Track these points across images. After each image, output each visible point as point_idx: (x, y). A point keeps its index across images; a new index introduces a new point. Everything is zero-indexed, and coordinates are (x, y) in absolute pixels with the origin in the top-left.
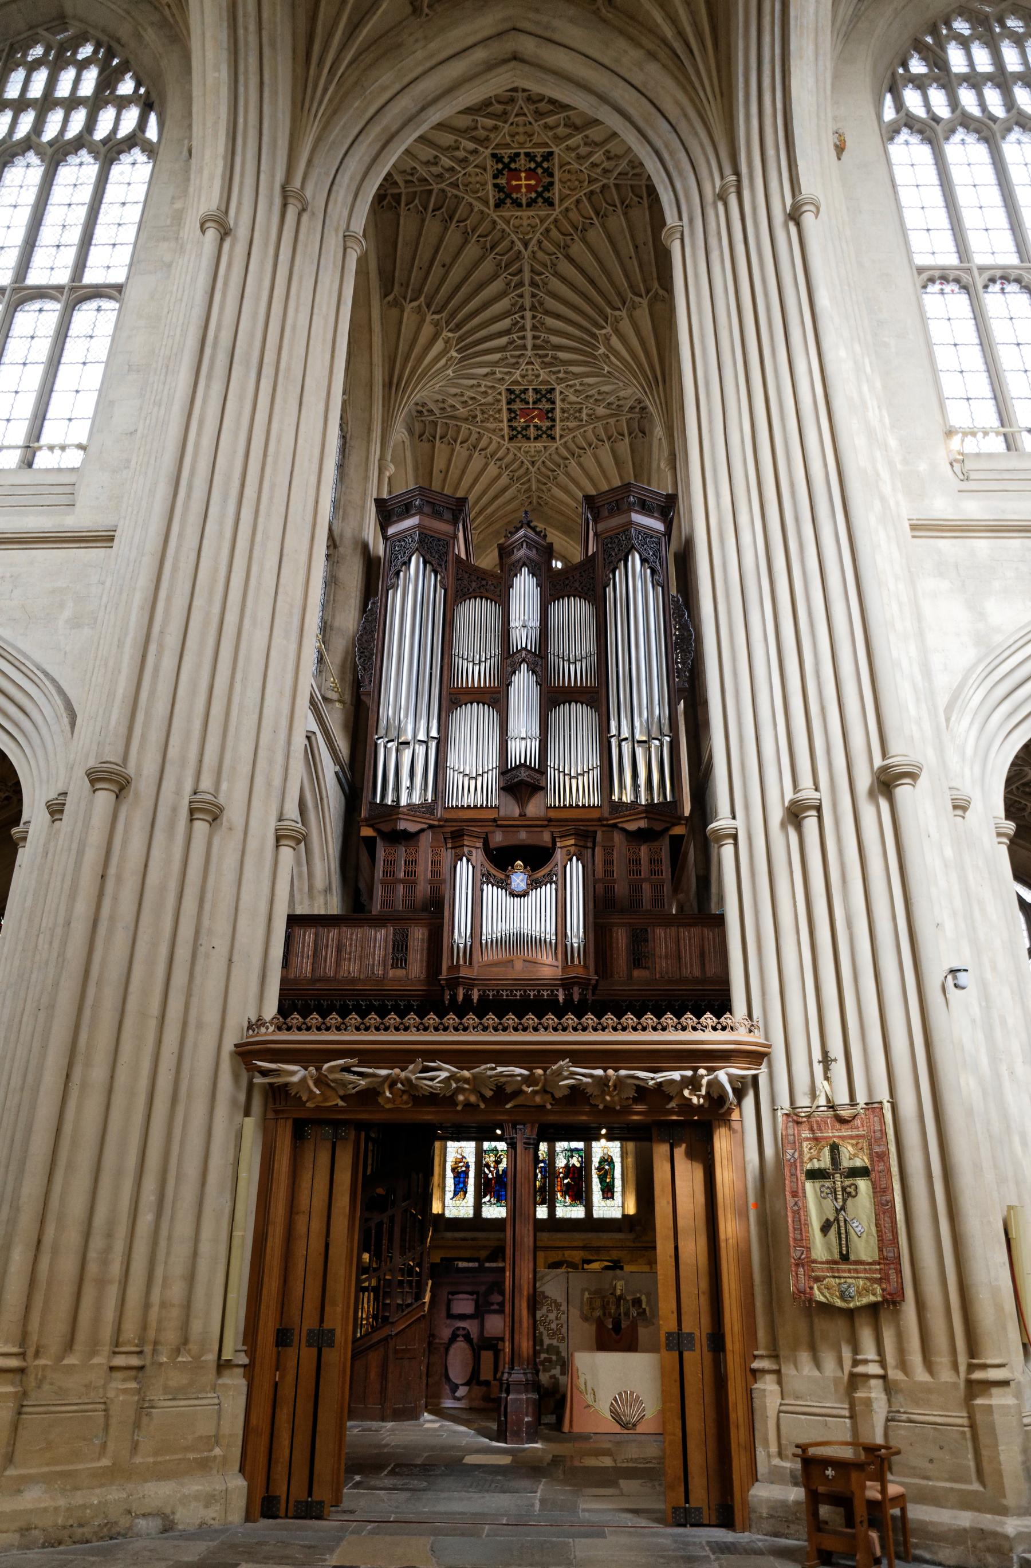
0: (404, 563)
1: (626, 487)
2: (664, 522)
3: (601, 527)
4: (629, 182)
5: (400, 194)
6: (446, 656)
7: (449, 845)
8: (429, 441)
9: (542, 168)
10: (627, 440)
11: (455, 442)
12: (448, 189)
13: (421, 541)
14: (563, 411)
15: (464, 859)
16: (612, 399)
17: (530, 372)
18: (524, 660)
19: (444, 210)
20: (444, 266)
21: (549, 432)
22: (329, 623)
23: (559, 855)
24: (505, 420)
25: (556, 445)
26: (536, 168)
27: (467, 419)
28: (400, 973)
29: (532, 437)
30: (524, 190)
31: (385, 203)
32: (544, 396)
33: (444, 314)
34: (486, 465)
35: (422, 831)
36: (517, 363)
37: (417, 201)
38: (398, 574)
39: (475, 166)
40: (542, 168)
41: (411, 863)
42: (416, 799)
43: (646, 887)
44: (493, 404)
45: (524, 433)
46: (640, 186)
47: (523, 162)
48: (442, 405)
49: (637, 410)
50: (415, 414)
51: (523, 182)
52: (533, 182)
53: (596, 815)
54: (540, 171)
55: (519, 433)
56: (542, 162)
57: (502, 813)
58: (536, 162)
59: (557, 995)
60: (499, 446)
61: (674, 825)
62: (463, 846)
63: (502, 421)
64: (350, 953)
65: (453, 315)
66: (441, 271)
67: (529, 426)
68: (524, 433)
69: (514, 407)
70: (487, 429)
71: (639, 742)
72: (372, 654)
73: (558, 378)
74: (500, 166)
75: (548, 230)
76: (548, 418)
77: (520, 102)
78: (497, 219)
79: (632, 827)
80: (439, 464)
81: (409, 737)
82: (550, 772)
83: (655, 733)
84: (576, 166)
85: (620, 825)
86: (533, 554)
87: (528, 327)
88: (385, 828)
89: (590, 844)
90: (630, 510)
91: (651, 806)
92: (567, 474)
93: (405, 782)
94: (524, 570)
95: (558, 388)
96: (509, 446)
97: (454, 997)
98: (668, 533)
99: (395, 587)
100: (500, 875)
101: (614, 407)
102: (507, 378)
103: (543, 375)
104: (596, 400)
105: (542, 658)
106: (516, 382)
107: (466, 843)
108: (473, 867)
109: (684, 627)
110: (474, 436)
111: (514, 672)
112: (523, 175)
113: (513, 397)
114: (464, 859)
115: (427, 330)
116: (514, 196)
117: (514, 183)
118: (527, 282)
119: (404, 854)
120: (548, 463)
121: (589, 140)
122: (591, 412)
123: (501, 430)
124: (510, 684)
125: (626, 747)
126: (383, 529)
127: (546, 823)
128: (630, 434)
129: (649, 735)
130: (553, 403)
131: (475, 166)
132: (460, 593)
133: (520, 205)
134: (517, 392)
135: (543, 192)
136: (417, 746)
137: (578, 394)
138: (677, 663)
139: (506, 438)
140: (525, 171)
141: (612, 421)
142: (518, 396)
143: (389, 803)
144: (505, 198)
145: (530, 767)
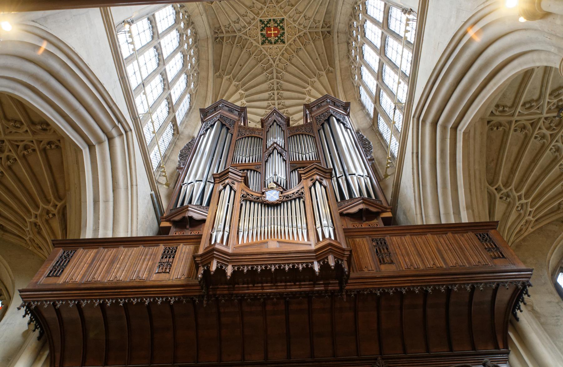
1: (326, 97)
4: (315, 30)
5: (223, 37)
9: (280, 26)
12: (243, 35)
18: (275, 148)
19: (241, 44)
20: (241, 66)
22: (168, 155)
26: (277, 26)
30: (273, 35)
31: (218, 40)
33: (240, 83)
37: (230, 40)
38: (207, 130)
39: (253, 26)
40: (280, 26)
46: (319, 32)
47: (272, 23)
51: (273, 32)
52: (276, 32)
54: (279, 27)
56: (280, 23)
58: (277, 23)
65: (244, 85)
66: (239, 67)
74: (263, 26)
75: (283, 54)
78: (262, 49)
84: (294, 25)
85: (345, 212)
87: (276, 99)
112: (272, 29)
115: (232, 88)
116: (269, 39)
117: (269, 32)
118: (275, 77)
121: (298, 11)
131: (253, 26)
133: (271, 43)
140: (273, 27)
144: (266, 39)
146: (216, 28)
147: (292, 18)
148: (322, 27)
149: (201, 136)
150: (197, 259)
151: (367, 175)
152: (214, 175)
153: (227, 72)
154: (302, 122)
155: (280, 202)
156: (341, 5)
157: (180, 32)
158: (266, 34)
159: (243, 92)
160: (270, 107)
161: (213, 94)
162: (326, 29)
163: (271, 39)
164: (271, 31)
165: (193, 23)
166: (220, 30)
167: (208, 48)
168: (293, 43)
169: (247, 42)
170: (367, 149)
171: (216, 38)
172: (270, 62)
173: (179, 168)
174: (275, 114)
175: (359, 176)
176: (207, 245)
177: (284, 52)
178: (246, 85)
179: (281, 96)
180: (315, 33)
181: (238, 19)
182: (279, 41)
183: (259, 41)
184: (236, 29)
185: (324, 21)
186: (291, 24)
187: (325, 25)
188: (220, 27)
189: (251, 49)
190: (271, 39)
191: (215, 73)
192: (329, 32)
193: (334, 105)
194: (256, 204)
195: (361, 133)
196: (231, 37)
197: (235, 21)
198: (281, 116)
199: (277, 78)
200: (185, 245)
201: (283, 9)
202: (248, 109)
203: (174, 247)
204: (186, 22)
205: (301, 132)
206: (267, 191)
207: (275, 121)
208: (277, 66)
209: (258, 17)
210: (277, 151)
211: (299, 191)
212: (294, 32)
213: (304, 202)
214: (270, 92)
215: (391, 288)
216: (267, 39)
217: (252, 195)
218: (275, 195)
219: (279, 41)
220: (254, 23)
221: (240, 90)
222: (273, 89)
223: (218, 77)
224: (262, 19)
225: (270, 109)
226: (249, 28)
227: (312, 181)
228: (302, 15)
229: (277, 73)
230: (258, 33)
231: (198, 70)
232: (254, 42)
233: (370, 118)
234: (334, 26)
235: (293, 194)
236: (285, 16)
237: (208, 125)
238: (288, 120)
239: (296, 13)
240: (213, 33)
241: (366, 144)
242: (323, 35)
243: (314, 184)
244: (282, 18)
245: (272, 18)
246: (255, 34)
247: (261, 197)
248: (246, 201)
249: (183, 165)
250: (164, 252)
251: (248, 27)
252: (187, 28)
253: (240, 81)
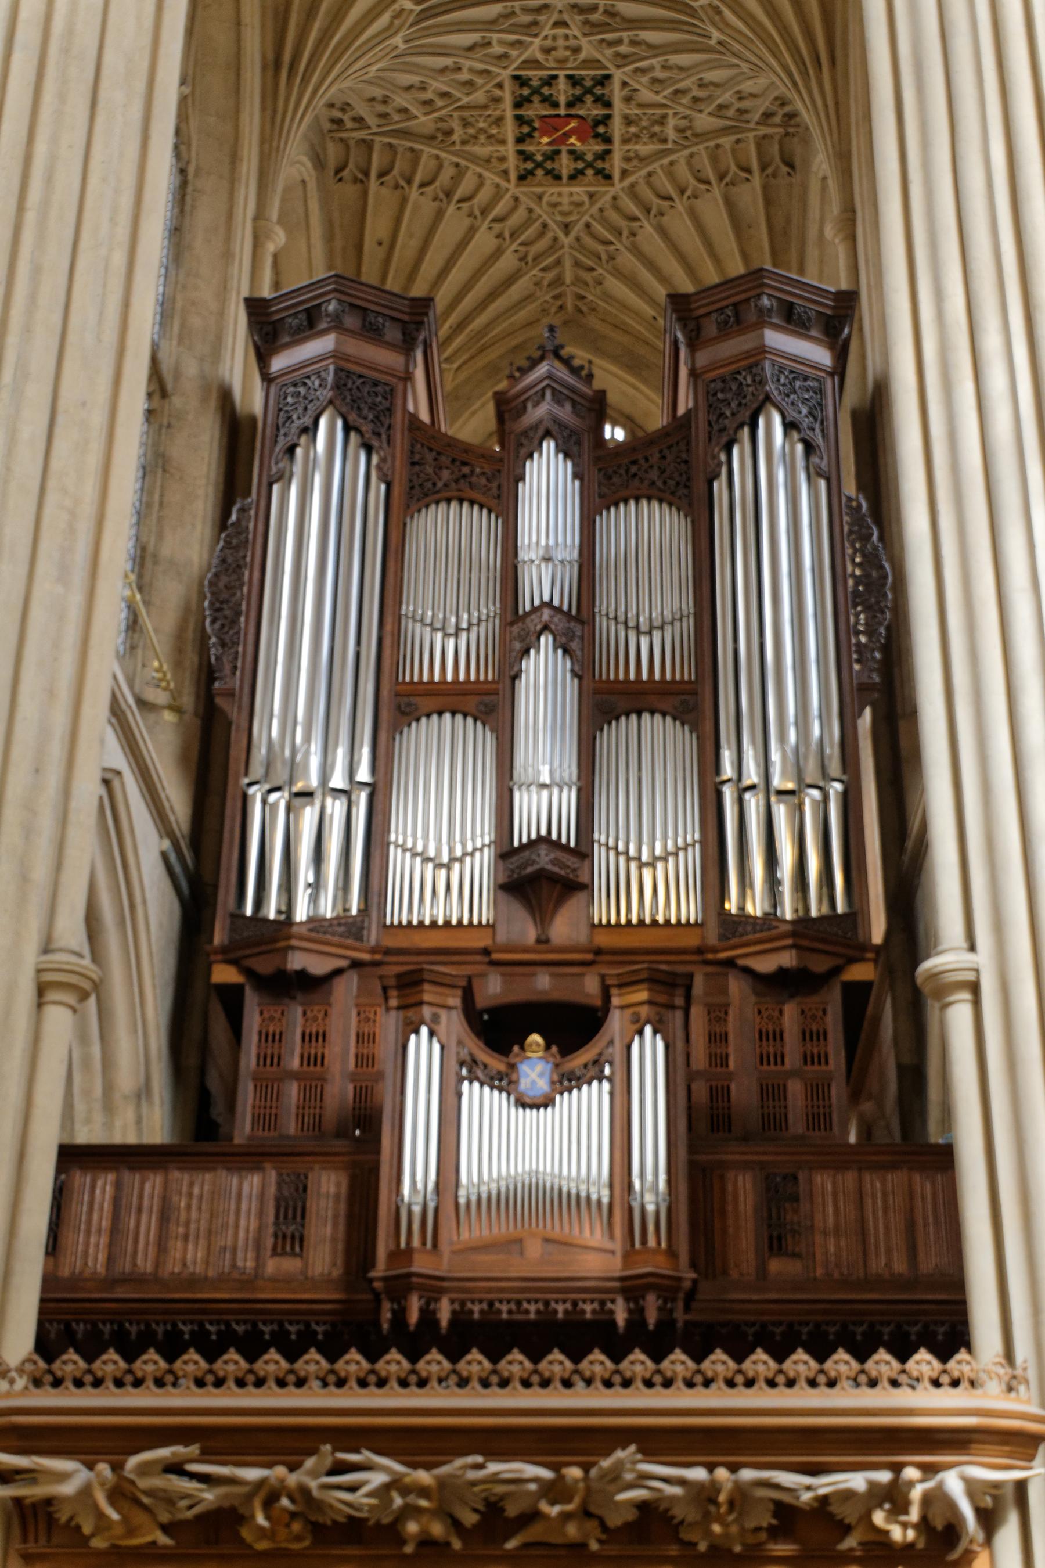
0: (305, 430)
1: (755, 277)
2: (831, 347)
3: (703, 358)
6: (389, 620)
7: (393, 1002)
8: (356, 180)
10: (757, 180)
11: (409, 182)
13: (338, 386)
14: (628, 121)
15: (424, 1031)
16: (726, 97)
17: (561, 42)
18: (546, 628)
21: (599, 165)
22: (151, 548)
23: (616, 1022)
24: (510, 139)
25: (612, 191)
27: (433, 138)
28: (290, 1265)
29: (565, 173)
32: (589, 91)
34: (472, 231)
35: (338, 972)
36: (535, 23)
38: (291, 450)
41: (315, 1037)
42: (327, 909)
43: (795, 1088)
44: (485, 107)
45: (549, 165)
48: (381, 108)
49: (777, 119)
50: (327, 126)
53: (691, 940)
55: (539, 165)
57: (502, 937)
59: (612, 1312)
60: (498, 193)
61: (852, 961)
62: (420, 1003)
63: (503, 142)
64: (187, 1224)
67: (558, 152)
68: (549, 165)
69: (528, 112)
70: (474, 159)
71: (780, 793)
72: (238, 614)
73: (617, 54)
76: (597, 135)
79: (765, 965)
80: (377, 227)
81: (314, 781)
82: (599, 854)
83: (811, 773)
85: (741, 962)
86: (565, 413)
88: (264, 966)
89: (679, 1001)
90: (762, 321)
91: (803, 923)
92: (636, 251)
93: (305, 873)
94: (549, 446)
95: (618, 75)
96: (520, 191)
97: (400, 1316)
98: (839, 370)
99: (283, 477)
100: (496, 1064)
101: (731, 113)
102: (514, 53)
103: (588, 49)
104: (696, 100)
105: (582, 623)
106: (532, 63)
107: (426, 997)
108: (442, 1048)
109: (871, 561)
110: (448, 172)
111: (526, 652)
113: (526, 92)
114: (424, 1031)
119: (300, 1020)
120: (598, 228)
122: (684, 123)
123: (502, 159)
124: (516, 676)
125: (753, 803)
126: (263, 358)
127: (589, 957)
128: (763, 168)
129: (800, 778)
130: (608, 105)
132: (417, 491)
134: (535, 83)
136: (329, 801)
137: (657, 87)
138: (857, 633)
139: (513, 176)
141: (727, 141)
142: (536, 91)
143: (272, 915)
145: (557, 845)
176: (392, 1246)
215: (780, 1323)
217: (485, 1066)
235: (585, 1066)
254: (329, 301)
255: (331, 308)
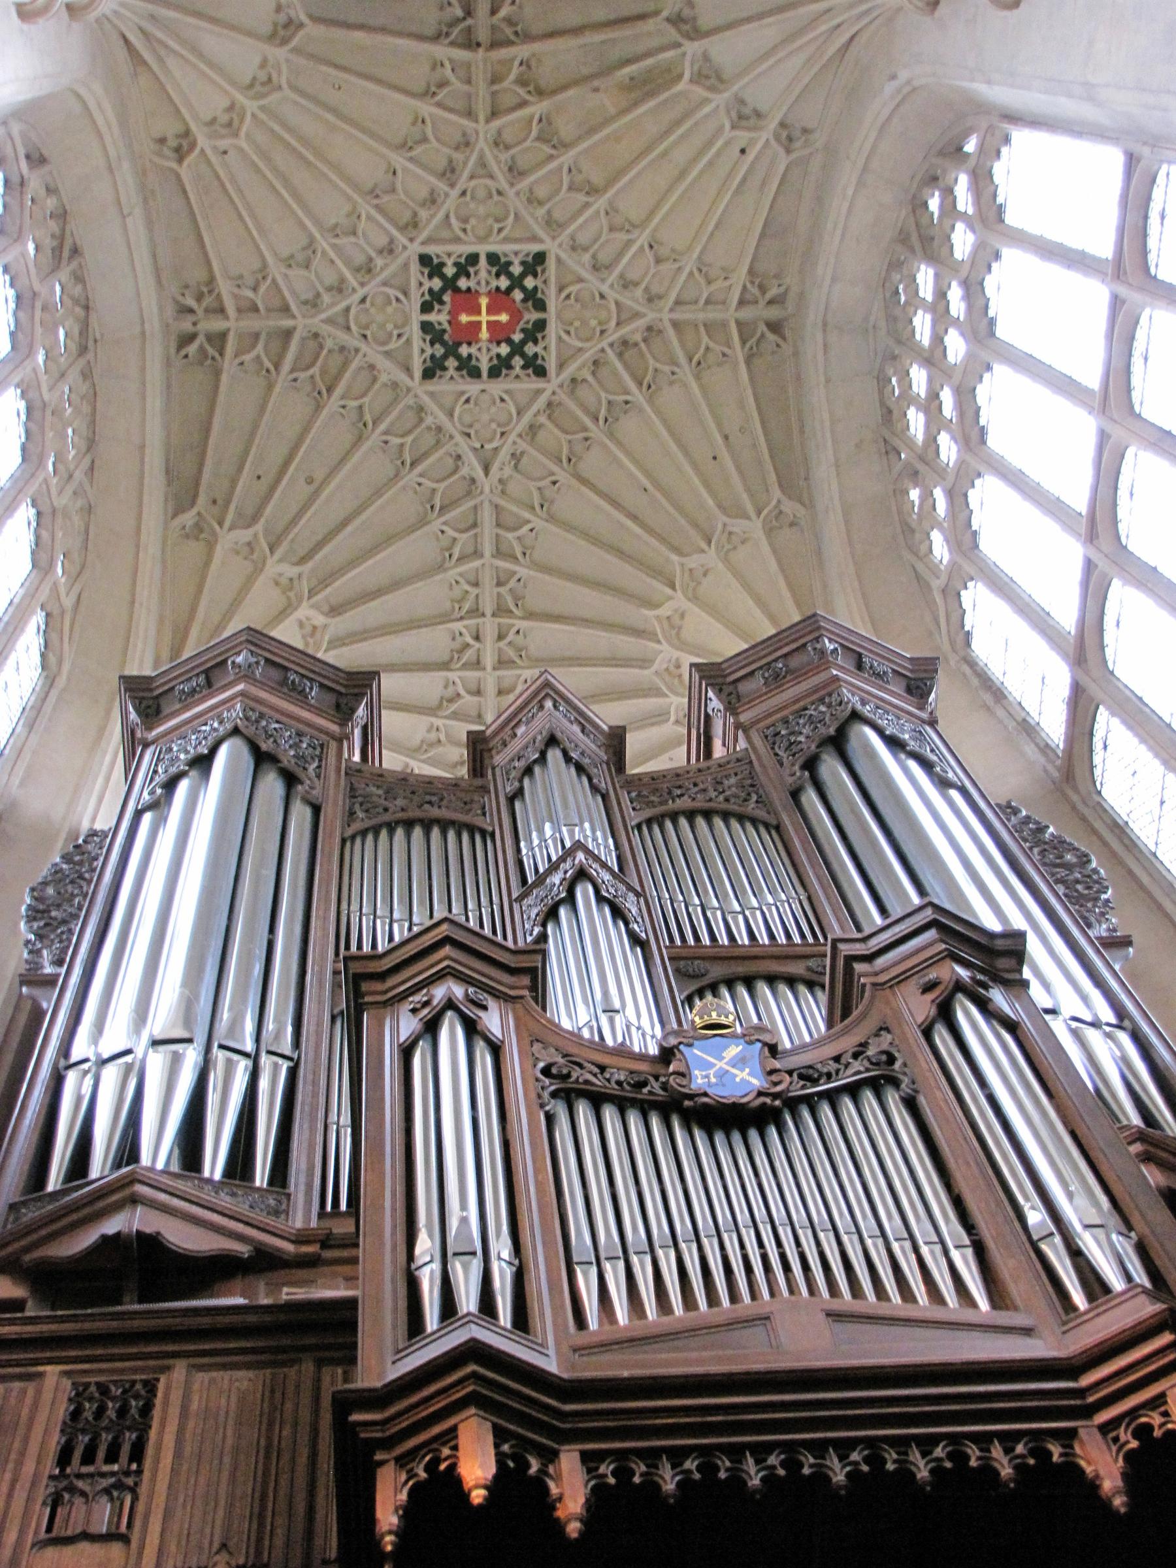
1: (811, 627)
4: (701, 316)
5: (223, 336)
9: (523, 289)
18: (582, 874)
19: (315, 370)
26: (509, 290)
30: (484, 334)
31: (192, 349)
37: (260, 348)
38: (170, 785)
39: (385, 284)
40: (523, 289)
46: (724, 325)
47: (483, 274)
51: (484, 318)
52: (504, 318)
54: (518, 295)
56: (523, 275)
58: (510, 275)
72: (77, 917)
74: (437, 283)
75: (533, 429)
77: (481, 144)
78: (426, 399)
84: (593, 282)
87: (489, 660)
112: (484, 302)
117: (464, 318)
118: (488, 549)
121: (618, 220)
133: (475, 373)
135: (523, 342)
146: (187, 287)
147: (585, 249)
148: (742, 303)
149: (139, 814)
150: (356, 1417)
151: (1113, 1021)
152: (351, 964)
153: (239, 514)
154: (677, 758)
155: (777, 1103)
156: (850, 192)
157: (23, 281)
158: (446, 326)
159: (319, 620)
160: (453, 707)
161: (161, 620)
162: (758, 312)
163: (473, 350)
164: (489, 312)
165: (75, 251)
166: (208, 301)
167: (144, 384)
168: (590, 378)
169: (345, 365)
170: (1079, 887)
171: (186, 339)
172: (464, 471)
173: (33, 978)
174: (549, 704)
175: (1074, 1024)
177: (542, 419)
178: (337, 584)
179: (519, 650)
180: (702, 329)
181: (354, 214)
182: (518, 361)
183: (410, 356)
184: (294, 293)
185: (751, 272)
186: (581, 280)
187: (755, 291)
188: (211, 280)
189: (366, 400)
190: (473, 350)
191: (175, 516)
192: (775, 327)
193: (860, 666)
194: (633, 1119)
195: (1024, 813)
196: (263, 337)
197: (292, 256)
198: (585, 723)
199: (499, 553)
200: (201, 1368)
201: (541, 203)
202: (390, 684)
203: (133, 1383)
204: (48, 243)
205: (700, 804)
206: (690, 1045)
207: (552, 741)
208: (503, 492)
209: (411, 240)
210: (597, 891)
211: (864, 1045)
212: (593, 323)
213: (911, 1104)
214: (458, 626)
216: (452, 350)
217: (603, 1068)
218: (740, 1062)
219: (518, 361)
220: (387, 268)
221: (305, 604)
222: (476, 612)
223: (187, 536)
224: (431, 250)
225: (455, 716)
226: (361, 293)
227: (930, 996)
228: (643, 239)
229: (498, 525)
230: (406, 321)
231: (87, 487)
232: (382, 363)
233: (1046, 749)
234: (802, 295)
235: (837, 1059)
236: (554, 238)
237: (173, 761)
238: (616, 741)
239: (612, 229)
240: (170, 311)
241: (1068, 867)
242: (744, 342)
243: (945, 1012)
244: (535, 248)
245: (483, 249)
246: (390, 327)
247: (657, 1078)
248: (568, 1096)
249: (59, 962)
250: (75, 1415)
251: (354, 290)
252: (56, 268)
253: (302, 560)
254: (238, 654)
255: (239, 659)
